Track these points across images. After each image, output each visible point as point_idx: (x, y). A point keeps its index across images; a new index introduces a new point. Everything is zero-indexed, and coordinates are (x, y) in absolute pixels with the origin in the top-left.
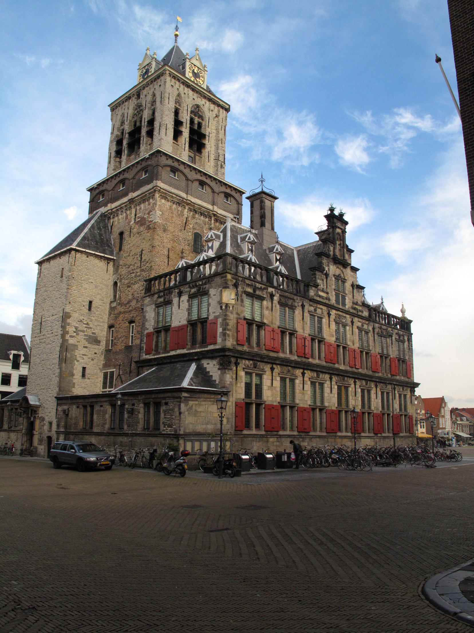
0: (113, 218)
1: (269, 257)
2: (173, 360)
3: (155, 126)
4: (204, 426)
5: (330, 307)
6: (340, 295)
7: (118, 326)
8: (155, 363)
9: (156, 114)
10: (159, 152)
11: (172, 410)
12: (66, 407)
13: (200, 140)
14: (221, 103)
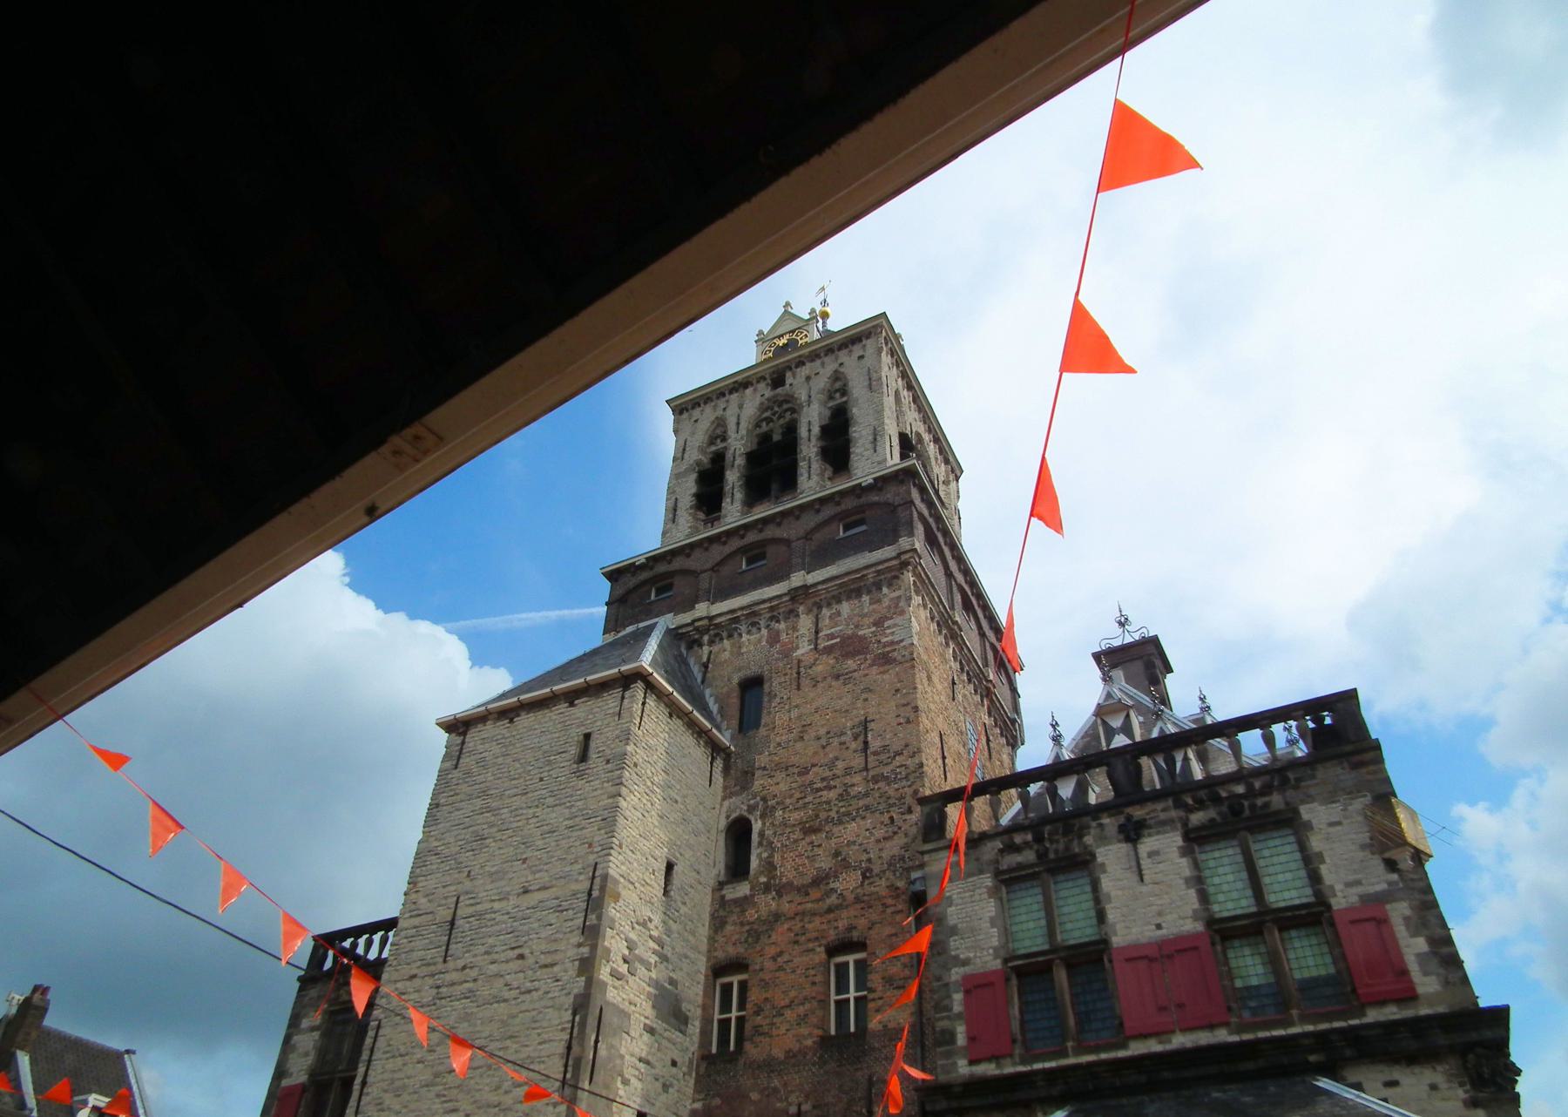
0: (711, 642)
7: (768, 964)
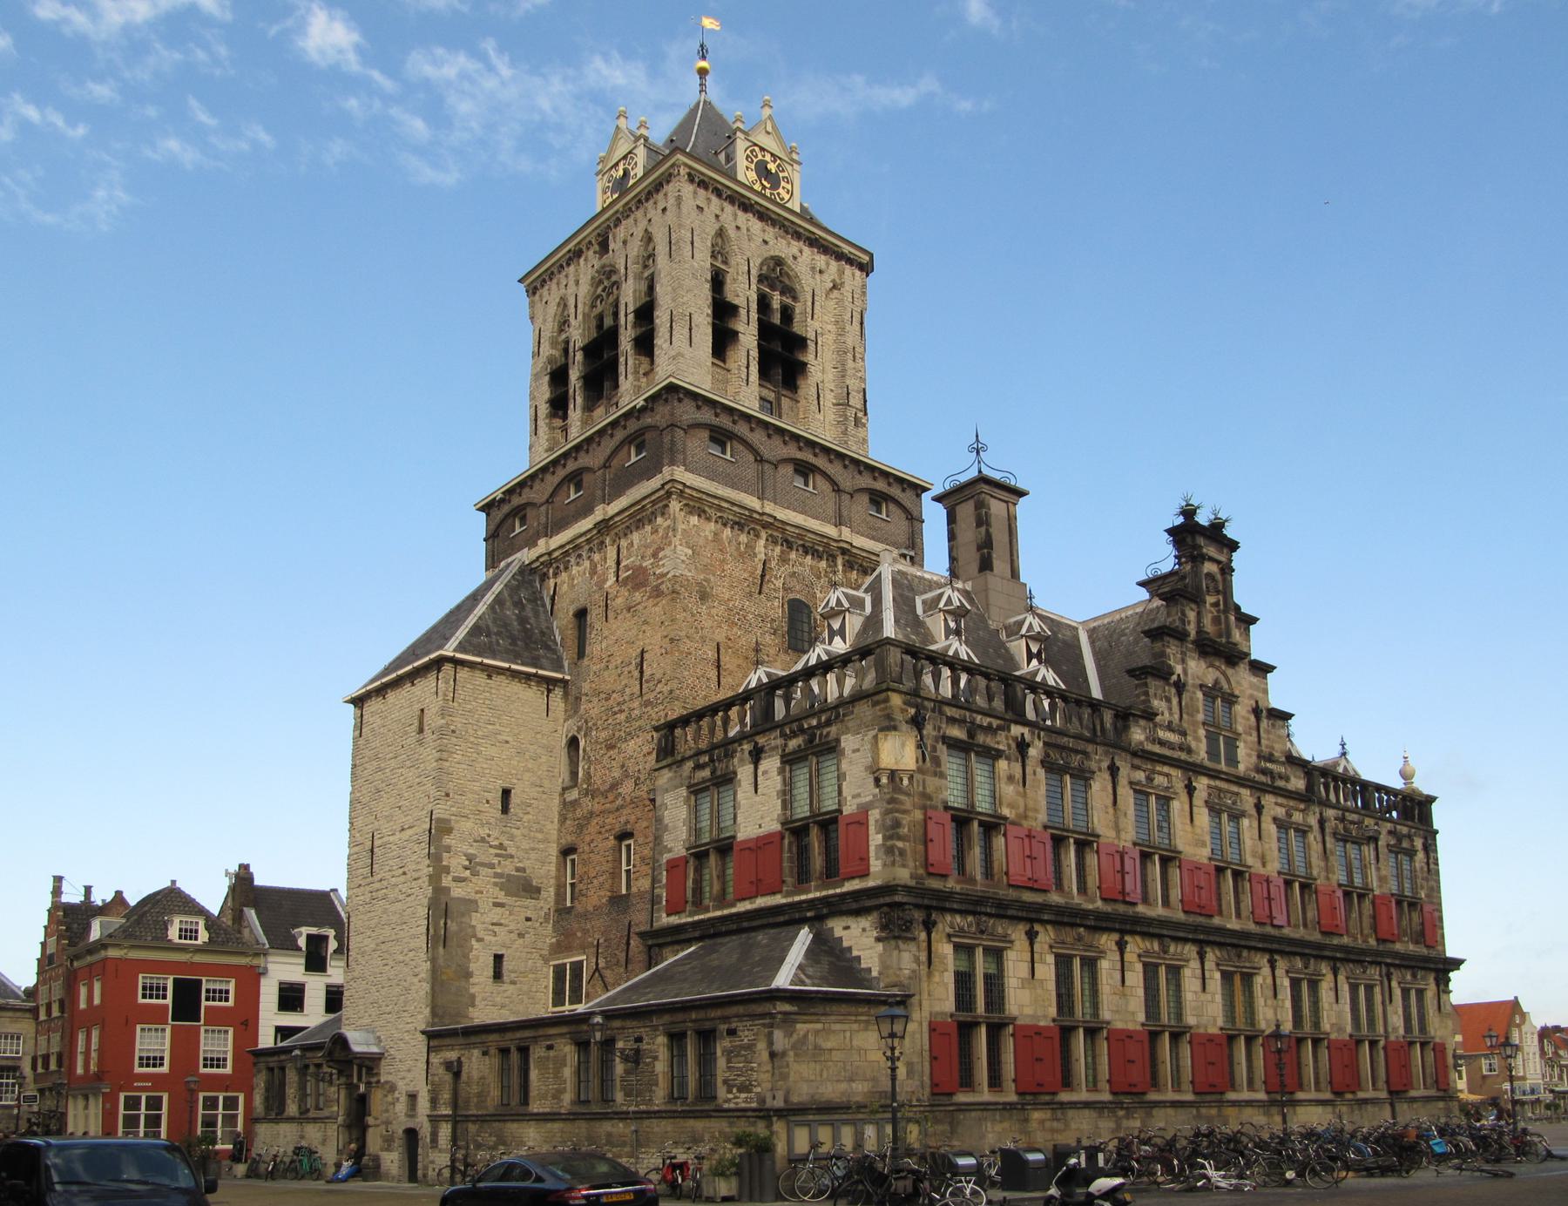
1: (1007, 650)
2: (745, 924)
3: (657, 321)
4: (843, 1086)
5: (1193, 769)
6: (1221, 737)
8: (697, 934)
9: (658, 288)
10: (672, 389)
12: (452, 1055)
13: (791, 352)
14: (846, 249)
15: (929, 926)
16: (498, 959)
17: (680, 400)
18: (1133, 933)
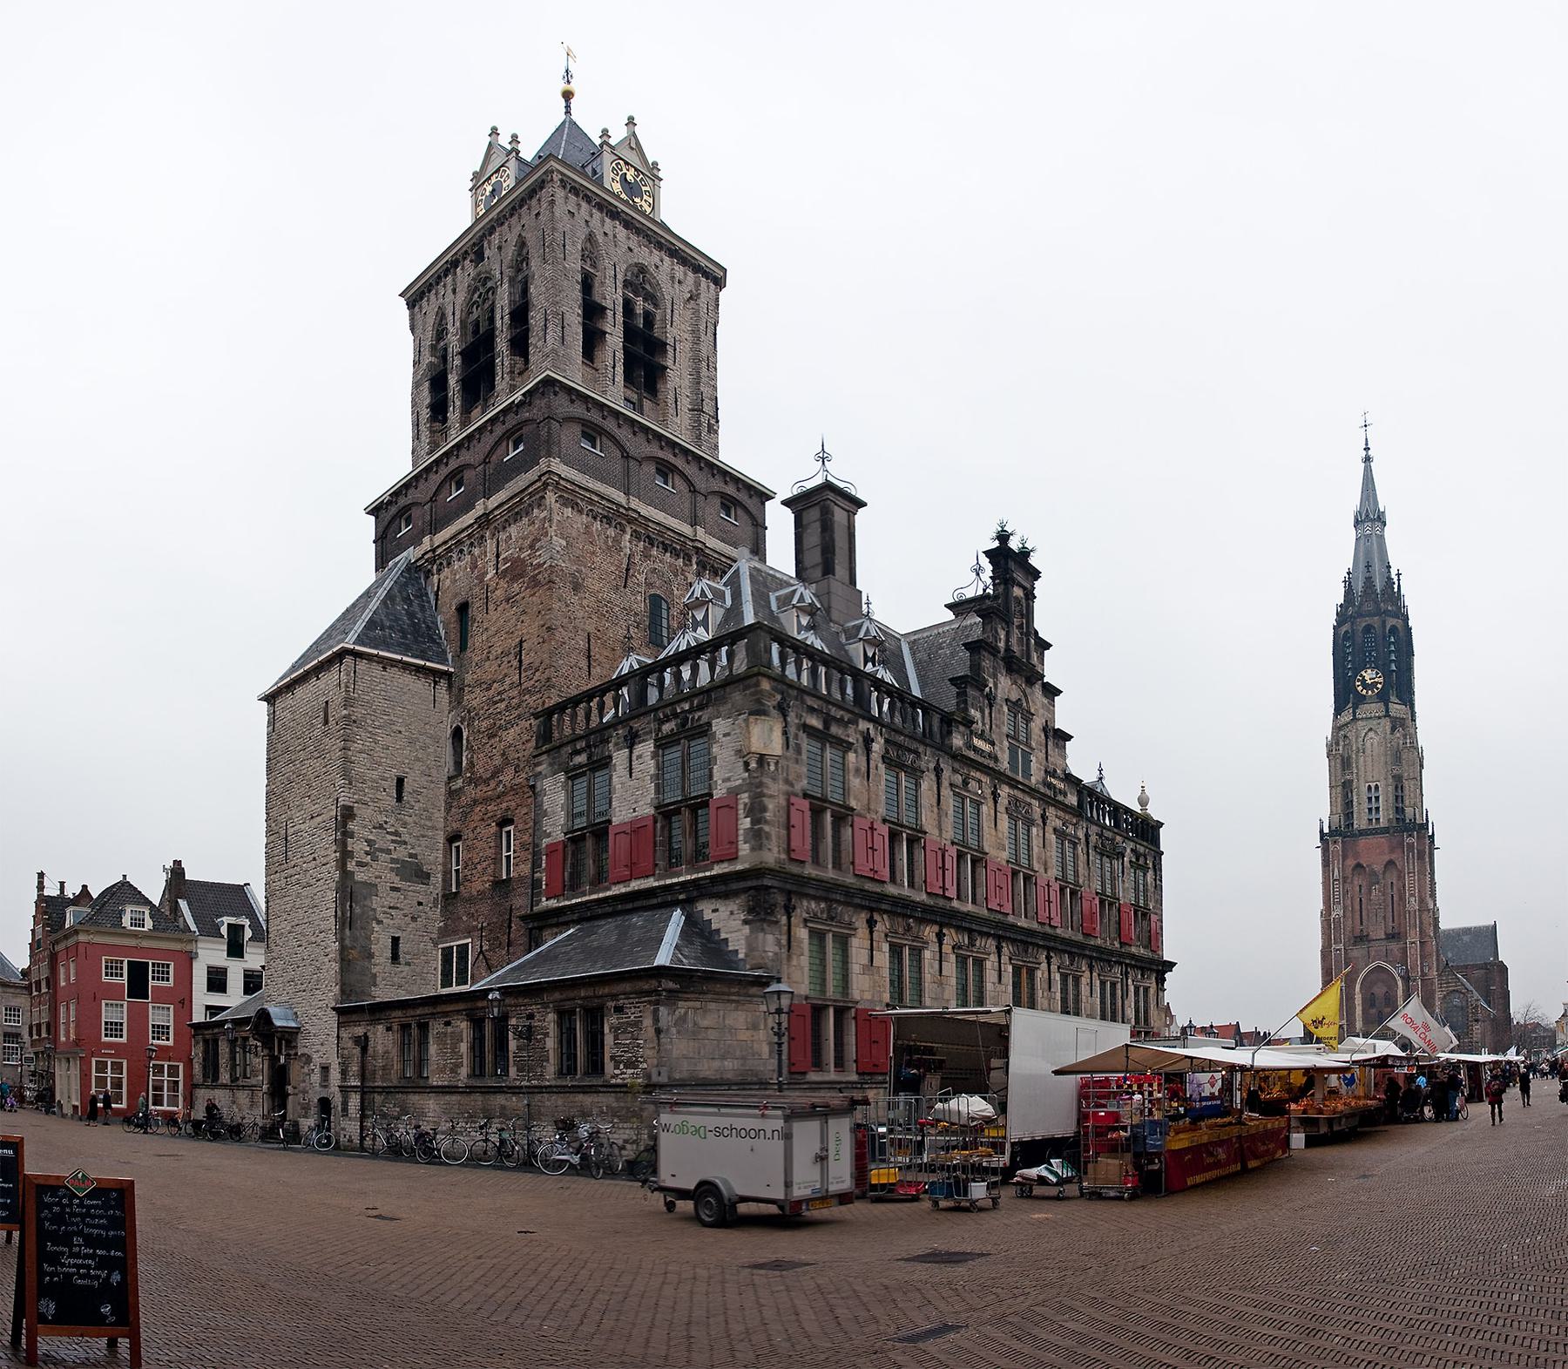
10: (549, 382)
11: (637, 1024)
12: (359, 1031)
14: (704, 263)
15: (789, 910)
16: (396, 941)
17: (556, 394)
18: (949, 925)
